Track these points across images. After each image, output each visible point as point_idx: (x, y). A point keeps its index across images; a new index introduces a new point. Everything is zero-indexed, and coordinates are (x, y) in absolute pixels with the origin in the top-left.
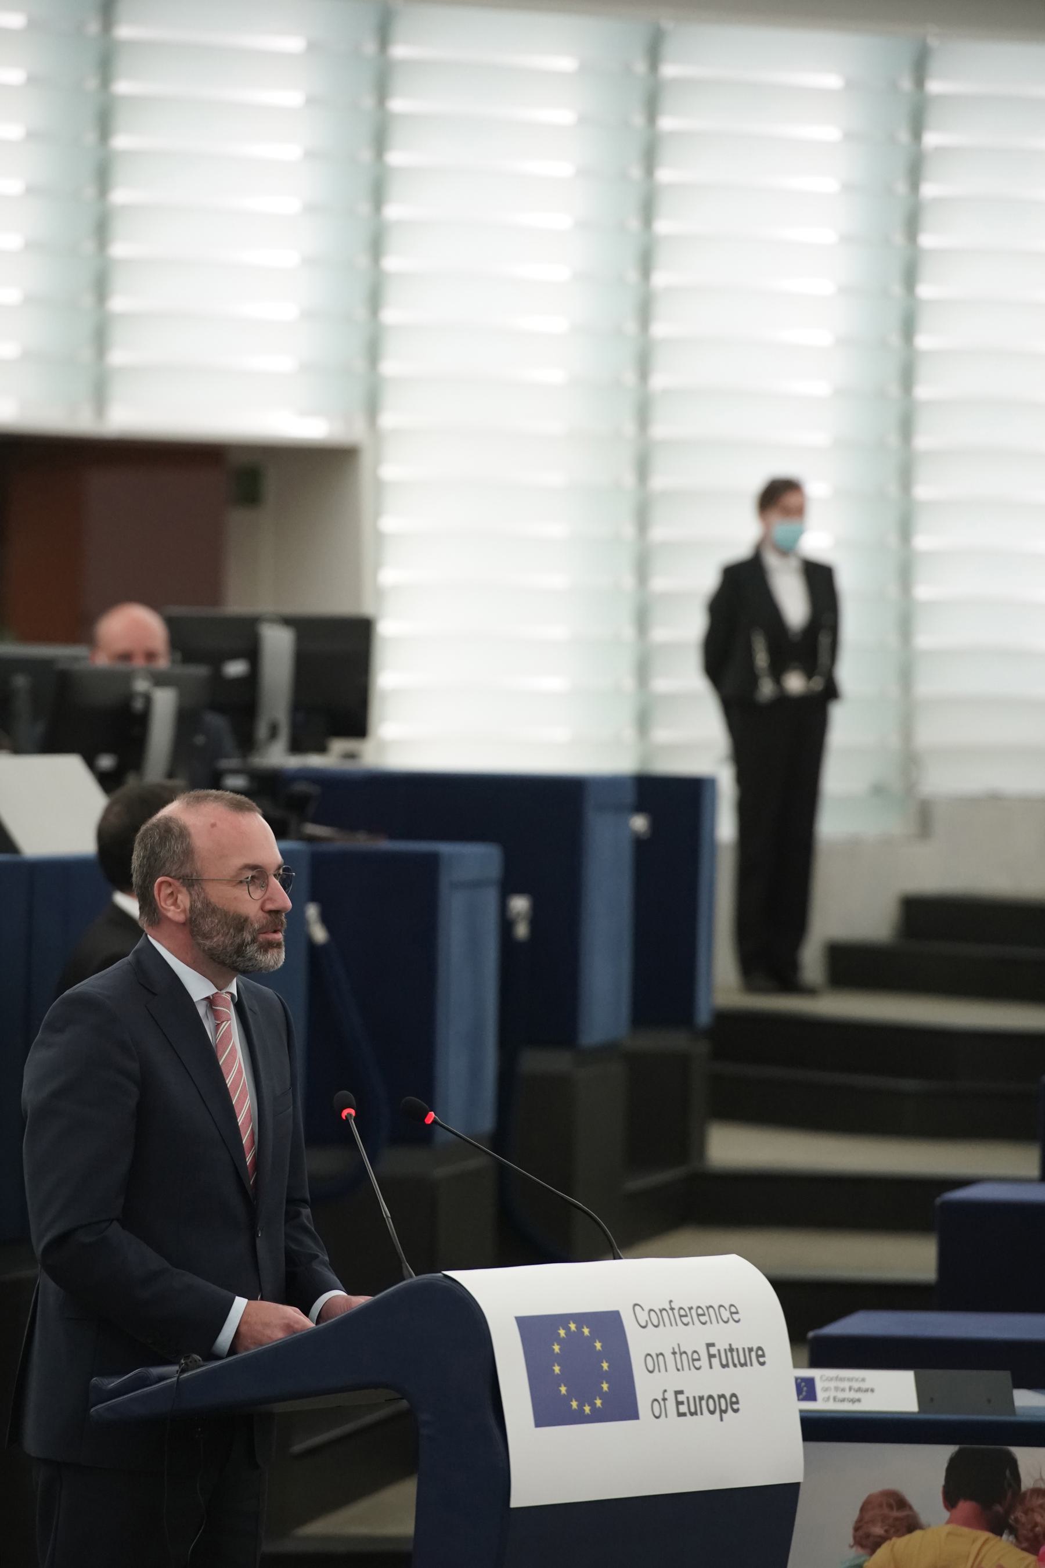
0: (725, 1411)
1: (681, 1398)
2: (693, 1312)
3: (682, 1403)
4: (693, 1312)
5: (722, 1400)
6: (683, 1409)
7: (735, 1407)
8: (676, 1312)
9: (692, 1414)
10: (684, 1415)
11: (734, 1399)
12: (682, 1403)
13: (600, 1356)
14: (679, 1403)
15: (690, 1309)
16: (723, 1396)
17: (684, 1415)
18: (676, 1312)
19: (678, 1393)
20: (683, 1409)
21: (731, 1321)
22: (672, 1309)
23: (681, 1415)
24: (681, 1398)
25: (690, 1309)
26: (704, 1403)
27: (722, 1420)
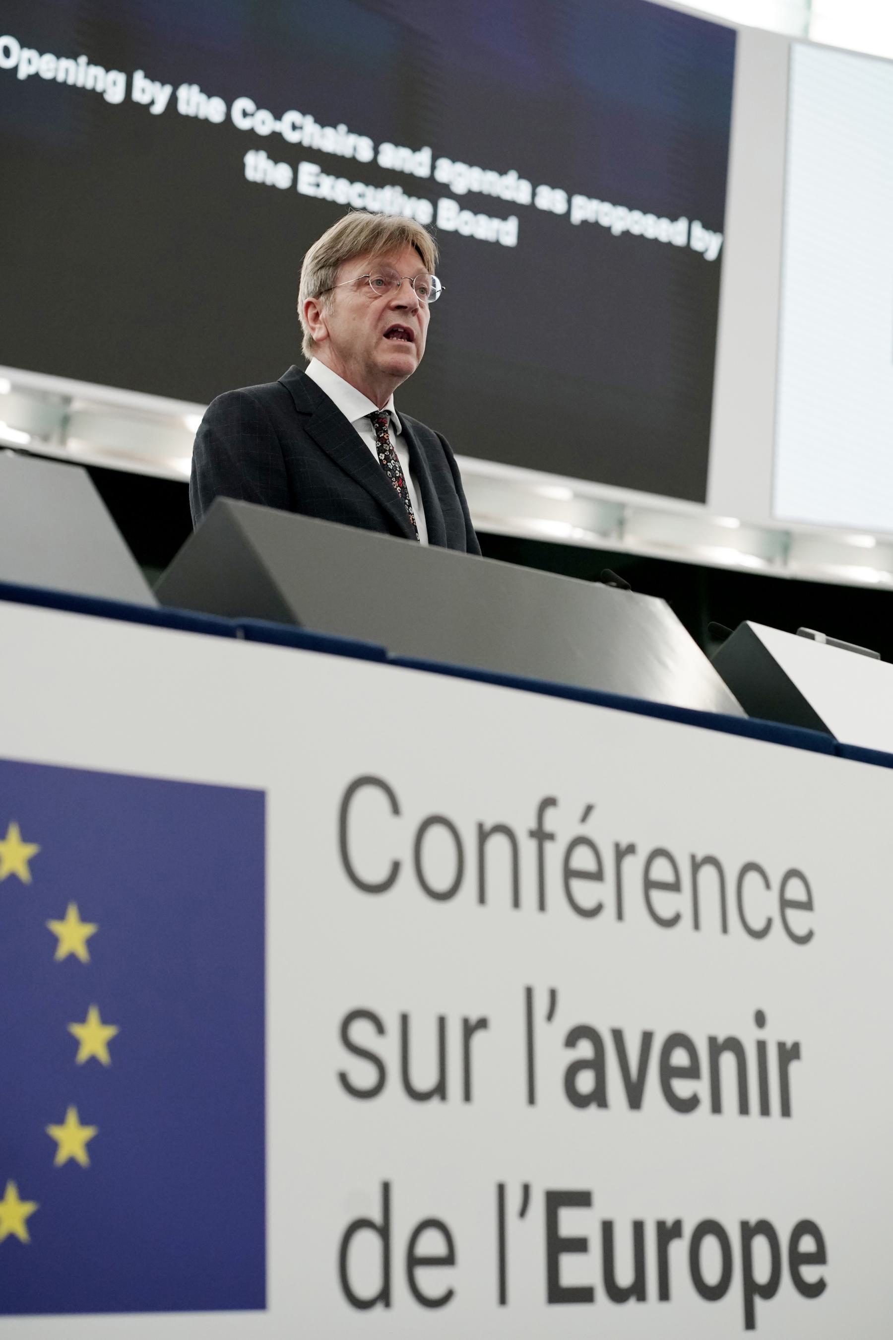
0: (770, 1290)
1: (572, 1222)
5: (760, 1244)
6: (578, 1270)
7: (810, 1274)
8: (554, 852)
9: (617, 1295)
10: (584, 1295)
14: (558, 1245)
15: (623, 852)
16: (765, 1228)
17: (584, 1295)
18: (554, 852)
20: (578, 1270)
22: (541, 835)
23: (558, 1294)
24: (572, 1222)
25: (623, 852)
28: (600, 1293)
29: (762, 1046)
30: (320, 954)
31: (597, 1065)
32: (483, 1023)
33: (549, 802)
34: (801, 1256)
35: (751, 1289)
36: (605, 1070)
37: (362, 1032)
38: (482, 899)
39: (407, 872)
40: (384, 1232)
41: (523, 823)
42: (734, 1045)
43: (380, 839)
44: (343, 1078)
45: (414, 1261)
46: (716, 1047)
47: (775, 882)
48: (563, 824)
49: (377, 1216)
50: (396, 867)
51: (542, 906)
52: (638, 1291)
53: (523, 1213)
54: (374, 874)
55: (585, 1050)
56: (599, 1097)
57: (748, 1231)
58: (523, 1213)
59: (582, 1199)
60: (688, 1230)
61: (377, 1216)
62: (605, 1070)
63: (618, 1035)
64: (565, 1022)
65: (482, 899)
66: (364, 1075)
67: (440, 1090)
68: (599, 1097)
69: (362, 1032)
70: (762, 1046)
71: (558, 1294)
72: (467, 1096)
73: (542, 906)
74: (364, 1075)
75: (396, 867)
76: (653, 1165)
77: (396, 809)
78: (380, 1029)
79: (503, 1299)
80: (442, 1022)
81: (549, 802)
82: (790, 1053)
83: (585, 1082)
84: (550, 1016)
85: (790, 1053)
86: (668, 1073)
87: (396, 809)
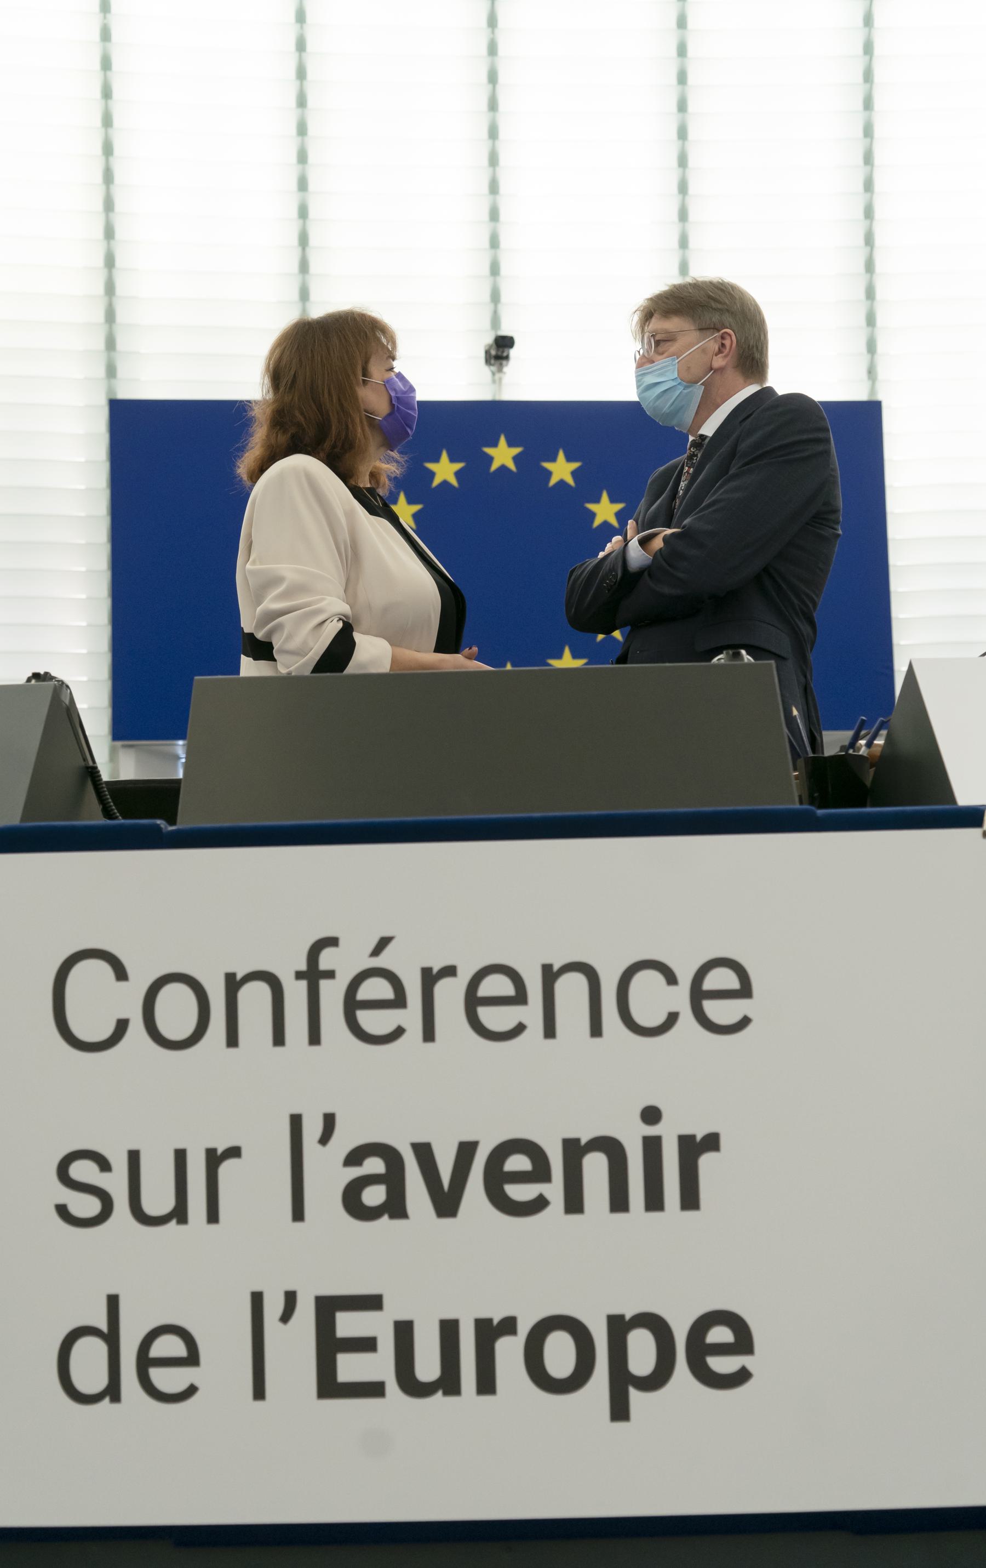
1: (348, 1324)
2: (450, 996)
3: (367, 1345)
4: (450, 996)
6: (350, 1367)
7: (721, 1365)
9: (412, 1386)
10: (375, 1390)
11: (720, 1334)
12: (367, 1345)
14: (329, 1346)
17: (375, 1390)
19: (327, 1308)
20: (350, 1367)
24: (348, 1324)
25: (429, 978)
26: (509, 1352)
27: (620, 1411)
28: (392, 1387)
29: (652, 1147)
31: (394, 1179)
32: (234, 1152)
36: (383, 1183)
37: (83, 1171)
39: (137, 1028)
40: (112, 1338)
41: (287, 966)
45: (145, 1362)
46: (574, 1151)
48: (343, 963)
49: (103, 1326)
51: (315, 1037)
52: (449, 1382)
53: (286, 1317)
54: (105, 1032)
55: (375, 1165)
56: (395, 1207)
57: (619, 1327)
58: (286, 1317)
59: (373, 1303)
60: (524, 1328)
61: (103, 1326)
62: (383, 1183)
63: (424, 1152)
64: (343, 1142)
66: (87, 1206)
67: (180, 1214)
68: (395, 1207)
69: (83, 1171)
70: (652, 1147)
71: (329, 1386)
72: (213, 1216)
73: (315, 1037)
74: (87, 1206)
77: (121, 973)
78: (104, 1165)
79: (259, 1392)
80: (180, 1156)
82: (694, 1148)
83: (374, 1196)
84: (325, 1139)
85: (694, 1148)
86: (496, 1181)
87: (121, 973)
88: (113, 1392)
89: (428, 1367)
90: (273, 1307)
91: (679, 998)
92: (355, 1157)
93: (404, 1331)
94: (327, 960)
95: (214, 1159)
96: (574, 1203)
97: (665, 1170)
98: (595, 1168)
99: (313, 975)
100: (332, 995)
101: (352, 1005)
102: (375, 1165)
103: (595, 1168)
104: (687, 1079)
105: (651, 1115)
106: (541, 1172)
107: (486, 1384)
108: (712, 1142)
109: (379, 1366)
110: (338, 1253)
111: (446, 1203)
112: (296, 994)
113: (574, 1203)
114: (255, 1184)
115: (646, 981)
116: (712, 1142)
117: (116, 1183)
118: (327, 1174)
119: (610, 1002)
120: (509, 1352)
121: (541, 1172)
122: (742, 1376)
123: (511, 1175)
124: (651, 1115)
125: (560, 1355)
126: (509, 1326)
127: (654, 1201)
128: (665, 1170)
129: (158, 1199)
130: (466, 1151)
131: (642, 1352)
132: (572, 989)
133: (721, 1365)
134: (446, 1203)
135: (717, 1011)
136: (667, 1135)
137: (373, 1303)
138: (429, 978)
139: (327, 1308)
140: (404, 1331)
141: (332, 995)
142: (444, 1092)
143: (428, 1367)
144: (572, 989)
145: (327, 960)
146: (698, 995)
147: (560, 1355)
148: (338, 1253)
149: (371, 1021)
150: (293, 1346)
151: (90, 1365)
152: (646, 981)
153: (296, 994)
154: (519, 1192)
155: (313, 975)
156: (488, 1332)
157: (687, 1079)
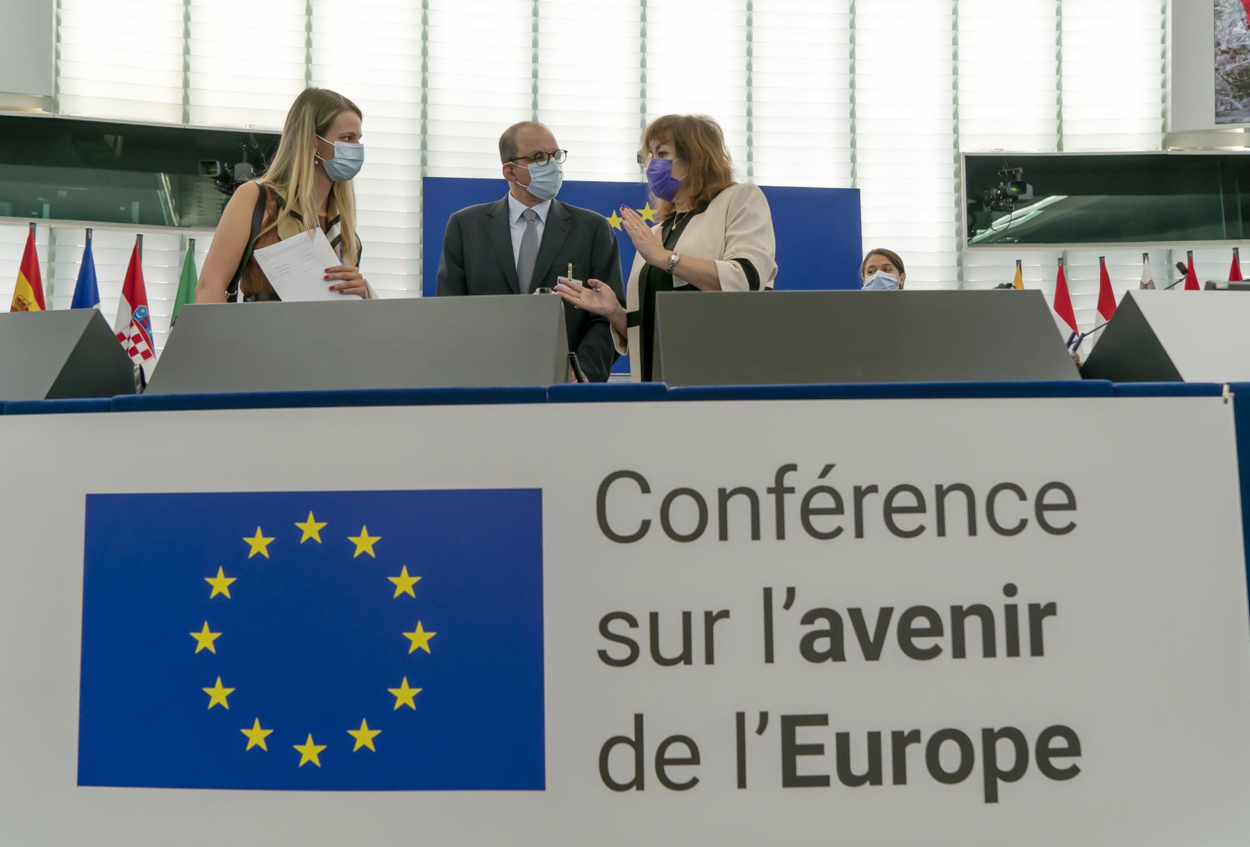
1: (804, 735)
2: (874, 505)
3: (818, 749)
4: (874, 505)
6: (806, 765)
7: (1059, 763)
9: (849, 779)
10: (823, 781)
11: (1058, 742)
12: (818, 749)
13: (408, 612)
14: (791, 750)
17: (823, 781)
19: (790, 723)
20: (806, 765)
21: (1033, 523)
24: (804, 735)
25: (859, 494)
29: (1011, 611)
30: (578, 583)
31: (836, 633)
32: (725, 614)
33: (793, 467)
34: (1055, 752)
35: (992, 775)
36: (830, 635)
38: (723, 536)
41: (762, 482)
42: (983, 612)
43: (628, 508)
44: (603, 655)
46: (959, 614)
47: (1032, 496)
48: (801, 481)
50: (646, 525)
51: (781, 535)
52: (874, 776)
53: (760, 730)
55: (822, 624)
56: (837, 653)
57: (990, 737)
58: (760, 730)
59: (822, 720)
60: (925, 738)
62: (828, 636)
63: (856, 614)
64: (802, 606)
65: (723, 536)
67: (686, 657)
68: (837, 653)
70: (1011, 611)
72: (710, 659)
73: (781, 535)
75: (646, 525)
76: (869, 696)
78: (633, 623)
80: (687, 617)
81: (793, 467)
82: (1040, 613)
83: (822, 645)
84: (788, 606)
85: (1040, 613)
86: (906, 634)
88: (638, 782)
89: (859, 765)
90: (752, 723)
91: (1027, 510)
92: (809, 618)
93: (843, 740)
94: (789, 480)
95: (710, 619)
96: (959, 651)
97: (1020, 628)
98: (973, 626)
99: (779, 490)
100: (793, 504)
101: (806, 512)
102: (822, 624)
103: (973, 626)
104: (1034, 565)
105: (1010, 590)
106: (936, 630)
107: (900, 777)
108: (1051, 609)
109: (826, 764)
110: (796, 685)
111: (872, 651)
112: (768, 504)
113: (959, 651)
114: (739, 637)
115: (1005, 497)
116: (1051, 609)
117: (641, 636)
118: (789, 629)
119: (982, 511)
120: (916, 755)
121: (936, 630)
122: (1073, 772)
123: (918, 631)
124: (1010, 590)
125: (950, 756)
126: (915, 736)
127: (1013, 650)
128: (1020, 628)
129: (671, 645)
130: (886, 614)
131: (1006, 755)
132: (956, 502)
133: (1059, 763)
134: (872, 651)
135: (1052, 518)
136: (1022, 602)
137: (822, 720)
138: (859, 494)
139: (790, 723)
140: (843, 740)
141: (793, 504)
142: (869, 572)
143: (859, 765)
144: (956, 502)
145: (789, 480)
146: (1040, 507)
147: (950, 756)
148: (796, 685)
149: (818, 522)
150: (766, 751)
151: (622, 764)
152: (1005, 497)
153: (768, 504)
154: (921, 643)
155: (779, 490)
156: (901, 741)
157: (1034, 565)
